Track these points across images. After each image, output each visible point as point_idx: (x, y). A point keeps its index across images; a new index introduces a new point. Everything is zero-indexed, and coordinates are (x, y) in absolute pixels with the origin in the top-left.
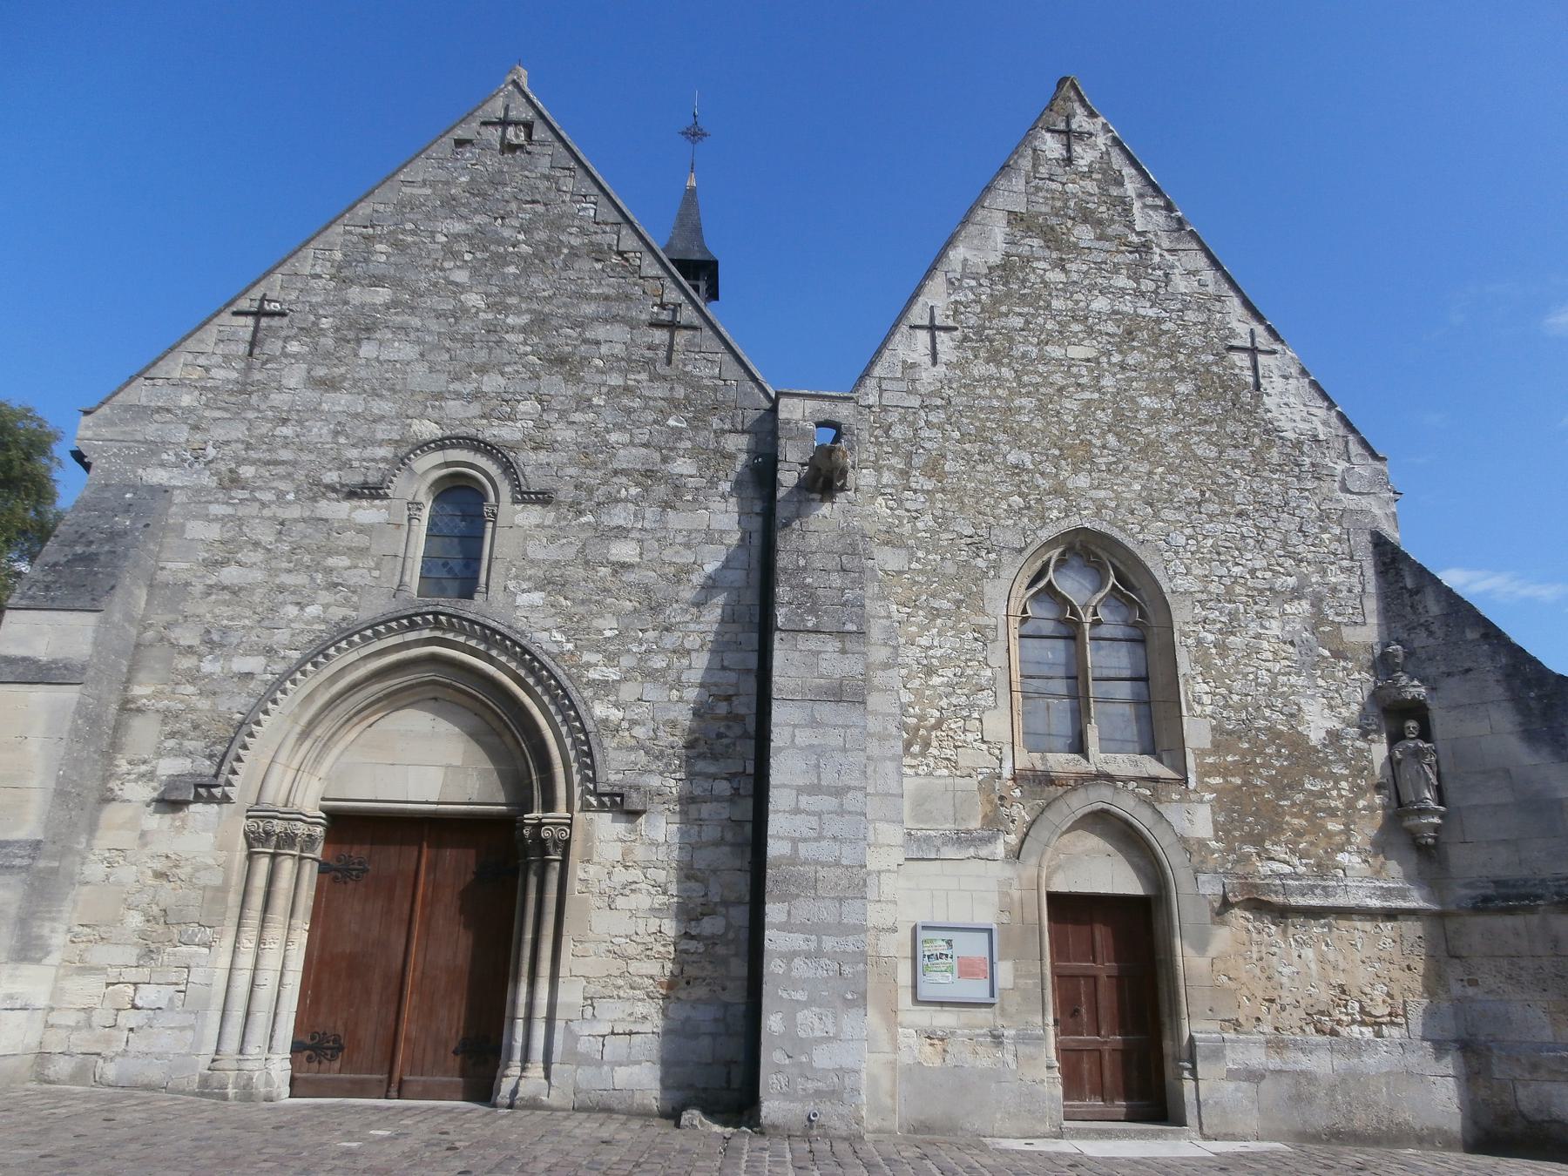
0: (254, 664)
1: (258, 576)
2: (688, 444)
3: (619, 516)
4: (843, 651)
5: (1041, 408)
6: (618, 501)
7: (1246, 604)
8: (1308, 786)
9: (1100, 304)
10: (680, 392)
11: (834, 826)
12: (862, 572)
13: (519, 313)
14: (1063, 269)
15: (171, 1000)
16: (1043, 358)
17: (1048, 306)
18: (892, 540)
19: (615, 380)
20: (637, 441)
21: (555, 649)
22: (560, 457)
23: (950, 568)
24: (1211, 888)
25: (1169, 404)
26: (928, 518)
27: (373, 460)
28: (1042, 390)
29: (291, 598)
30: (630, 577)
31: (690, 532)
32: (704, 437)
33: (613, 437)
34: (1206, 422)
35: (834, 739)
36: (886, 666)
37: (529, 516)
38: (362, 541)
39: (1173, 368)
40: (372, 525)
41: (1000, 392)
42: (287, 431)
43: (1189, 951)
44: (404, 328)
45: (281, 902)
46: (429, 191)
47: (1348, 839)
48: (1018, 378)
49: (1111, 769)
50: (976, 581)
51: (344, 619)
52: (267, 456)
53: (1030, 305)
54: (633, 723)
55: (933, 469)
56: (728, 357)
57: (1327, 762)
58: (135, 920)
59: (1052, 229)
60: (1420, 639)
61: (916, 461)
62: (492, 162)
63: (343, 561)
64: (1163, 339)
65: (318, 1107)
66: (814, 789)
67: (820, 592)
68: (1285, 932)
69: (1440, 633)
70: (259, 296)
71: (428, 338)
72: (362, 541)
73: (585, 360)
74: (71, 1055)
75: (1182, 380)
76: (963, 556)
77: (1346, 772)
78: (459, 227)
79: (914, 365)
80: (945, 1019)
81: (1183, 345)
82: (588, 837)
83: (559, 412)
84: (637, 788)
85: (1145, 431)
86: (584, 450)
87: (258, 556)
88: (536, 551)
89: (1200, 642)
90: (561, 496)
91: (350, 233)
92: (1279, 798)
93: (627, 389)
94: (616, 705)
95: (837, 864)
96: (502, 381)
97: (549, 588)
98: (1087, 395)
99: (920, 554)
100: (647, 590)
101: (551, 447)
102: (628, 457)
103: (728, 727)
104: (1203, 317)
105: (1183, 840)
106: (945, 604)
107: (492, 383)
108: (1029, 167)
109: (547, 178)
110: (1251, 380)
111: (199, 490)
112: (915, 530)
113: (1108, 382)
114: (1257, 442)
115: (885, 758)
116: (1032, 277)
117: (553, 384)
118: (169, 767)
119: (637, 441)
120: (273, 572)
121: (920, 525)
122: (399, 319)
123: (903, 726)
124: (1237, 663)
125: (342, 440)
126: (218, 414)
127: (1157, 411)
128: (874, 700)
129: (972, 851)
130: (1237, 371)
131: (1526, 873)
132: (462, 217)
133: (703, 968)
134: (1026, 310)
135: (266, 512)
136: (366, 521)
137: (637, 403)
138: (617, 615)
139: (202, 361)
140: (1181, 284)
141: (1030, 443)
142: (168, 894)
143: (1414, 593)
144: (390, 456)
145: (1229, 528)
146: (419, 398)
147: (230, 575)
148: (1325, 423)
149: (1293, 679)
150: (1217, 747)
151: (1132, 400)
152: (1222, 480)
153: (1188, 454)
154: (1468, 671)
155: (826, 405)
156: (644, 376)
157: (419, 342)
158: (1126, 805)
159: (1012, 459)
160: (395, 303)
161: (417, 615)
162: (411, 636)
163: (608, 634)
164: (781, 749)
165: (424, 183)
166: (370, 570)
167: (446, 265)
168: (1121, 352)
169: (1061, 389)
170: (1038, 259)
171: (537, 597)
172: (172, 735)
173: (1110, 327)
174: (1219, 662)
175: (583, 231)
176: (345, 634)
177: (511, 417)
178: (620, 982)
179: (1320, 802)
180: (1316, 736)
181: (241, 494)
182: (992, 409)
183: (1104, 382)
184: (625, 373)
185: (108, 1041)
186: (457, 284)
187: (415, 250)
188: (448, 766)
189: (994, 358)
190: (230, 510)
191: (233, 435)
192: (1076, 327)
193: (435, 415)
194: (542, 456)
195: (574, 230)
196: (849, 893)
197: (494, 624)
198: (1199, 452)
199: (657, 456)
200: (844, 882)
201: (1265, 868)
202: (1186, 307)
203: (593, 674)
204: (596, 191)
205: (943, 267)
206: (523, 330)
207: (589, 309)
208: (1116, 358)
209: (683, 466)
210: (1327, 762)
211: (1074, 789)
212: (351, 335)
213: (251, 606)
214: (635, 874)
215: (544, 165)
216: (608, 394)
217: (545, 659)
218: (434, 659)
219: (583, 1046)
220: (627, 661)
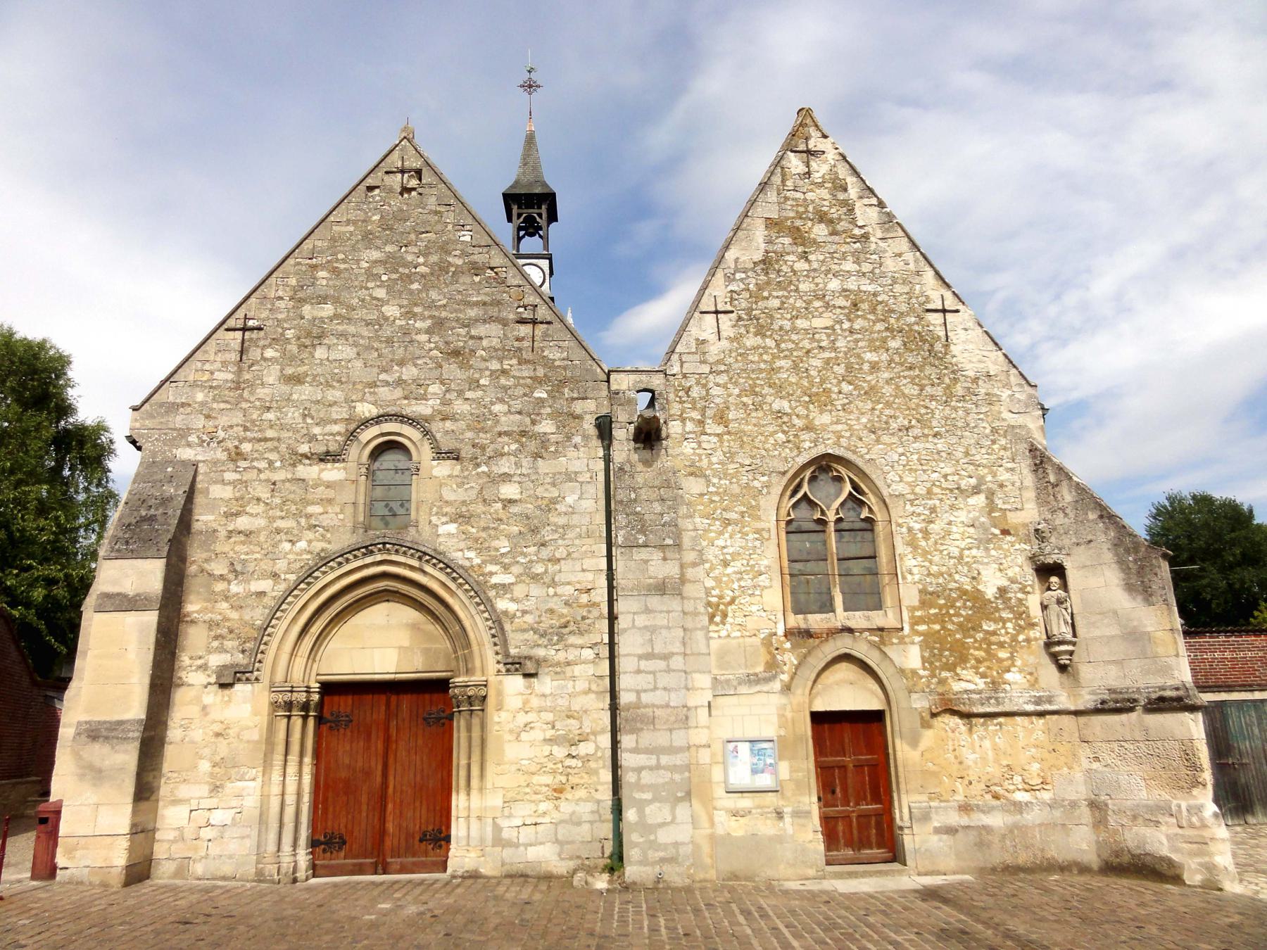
0: (265, 585)
1: (262, 522)
2: (549, 410)
3: (504, 466)
4: (665, 559)
5: (795, 367)
6: (502, 455)
7: (941, 500)
8: (985, 627)
9: (834, 284)
10: (541, 372)
11: (664, 680)
12: (675, 499)
13: (424, 319)
14: (807, 259)
15: (233, 819)
16: (794, 329)
17: (797, 290)
18: (696, 472)
19: (495, 365)
20: (513, 410)
21: (467, 564)
22: (462, 425)
23: (736, 489)
24: (921, 703)
25: (885, 357)
26: (719, 453)
28: (795, 354)
29: (284, 537)
30: (515, 509)
31: (554, 474)
32: (561, 404)
33: (497, 408)
34: (910, 368)
35: (661, 620)
36: (694, 565)
37: (443, 469)
38: (330, 494)
39: (887, 329)
40: (335, 482)
41: (765, 357)
42: (270, 416)
43: (906, 748)
44: (343, 335)
45: (295, 747)
46: (351, 228)
48: (778, 345)
49: (852, 624)
50: (754, 497)
51: (323, 550)
52: (259, 435)
53: (785, 289)
54: (524, 612)
55: (721, 418)
56: (573, 344)
57: (997, 610)
58: (205, 766)
59: (798, 229)
60: (1060, 519)
61: (709, 413)
62: (396, 202)
63: (316, 509)
64: (879, 307)
65: (335, 885)
66: (649, 656)
67: (646, 517)
68: (970, 730)
69: (1072, 515)
70: (242, 316)
71: (362, 342)
72: (330, 494)
73: (473, 351)
74: (174, 860)
75: (893, 338)
76: (744, 480)
78: (376, 255)
79: (704, 342)
80: (745, 802)
81: (893, 311)
82: (500, 693)
84: (530, 658)
85: (868, 378)
86: (480, 419)
87: (260, 508)
88: (448, 495)
89: (910, 530)
90: (463, 454)
91: (299, 264)
92: (965, 637)
93: (504, 372)
94: (512, 600)
95: (667, 706)
96: (414, 371)
98: (827, 355)
99: (715, 480)
100: (528, 518)
102: (508, 422)
103: (589, 612)
104: (906, 289)
105: (902, 671)
106: (733, 516)
107: (409, 372)
108: (779, 183)
109: (436, 213)
110: (942, 334)
111: (215, 463)
112: (711, 463)
113: (841, 343)
114: (947, 380)
115: (697, 629)
116: (784, 268)
117: (452, 370)
118: (216, 660)
119: (513, 410)
120: (272, 519)
121: (714, 460)
122: (340, 328)
123: (709, 604)
124: (936, 543)
125: (309, 421)
126: (222, 406)
127: (877, 363)
128: (689, 589)
129: (758, 688)
130: (931, 328)
131: (1128, 683)
132: (378, 248)
133: (582, 778)
134: (781, 293)
135: (262, 476)
137: (511, 382)
138: (508, 537)
139: (207, 367)
140: (891, 265)
141: (789, 394)
142: (223, 748)
143: (1055, 486)
144: (343, 430)
145: (928, 445)
146: (359, 387)
147: (242, 523)
148: (995, 363)
149: (974, 552)
150: (924, 604)
151: (858, 356)
152: (923, 411)
153: (899, 393)
154: (1090, 541)
155: (644, 377)
156: (514, 361)
157: (355, 345)
158: (860, 649)
159: (776, 406)
160: (336, 316)
162: (369, 560)
163: (503, 551)
164: (625, 630)
165: (348, 222)
167: (370, 285)
168: (849, 320)
169: (808, 352)
170: (788, 254)
171: (452, 528)
172: (216, 638)
173: (841, 302)
174: (923, 543)
175: (464, 254)
176: (325, 561)
177: (424, 397)
178: (527, 790)
179: (993, 639)
180: (990, 592)
181: (243, 464)
182: (761, 371)
183: (838, 344)
184: (501, 360)
185: (196, 849)
186: (378, 299)
187: (346, 275)
188: (400, 648)
189: (760, 332)
190: (238, 476)
191: (235, 421)
192: (817, 304)
193: (372, 399)
194: (448, 424)
195: (458, 253)
196: (676, 726)
197: (423, 549)
198: (906, 391)
199: (528, 420)
200: (673, 718)
201: (957, 687)
202: (894, 281)
203: (494, 580)
204: (470, 221)
205: (722, 266)
206: (429, 331)
207: (472, 313)
208: (846, 325)
209: (547, 427)
210: (997, 610)
211: (827, 640)
212: (308, 342)
213: (259, 544)
214: (531, 717)
215: (432, 202)
216: (491, 375)
217: (461, 571)
219: (505, 834)
220: (516, 570)
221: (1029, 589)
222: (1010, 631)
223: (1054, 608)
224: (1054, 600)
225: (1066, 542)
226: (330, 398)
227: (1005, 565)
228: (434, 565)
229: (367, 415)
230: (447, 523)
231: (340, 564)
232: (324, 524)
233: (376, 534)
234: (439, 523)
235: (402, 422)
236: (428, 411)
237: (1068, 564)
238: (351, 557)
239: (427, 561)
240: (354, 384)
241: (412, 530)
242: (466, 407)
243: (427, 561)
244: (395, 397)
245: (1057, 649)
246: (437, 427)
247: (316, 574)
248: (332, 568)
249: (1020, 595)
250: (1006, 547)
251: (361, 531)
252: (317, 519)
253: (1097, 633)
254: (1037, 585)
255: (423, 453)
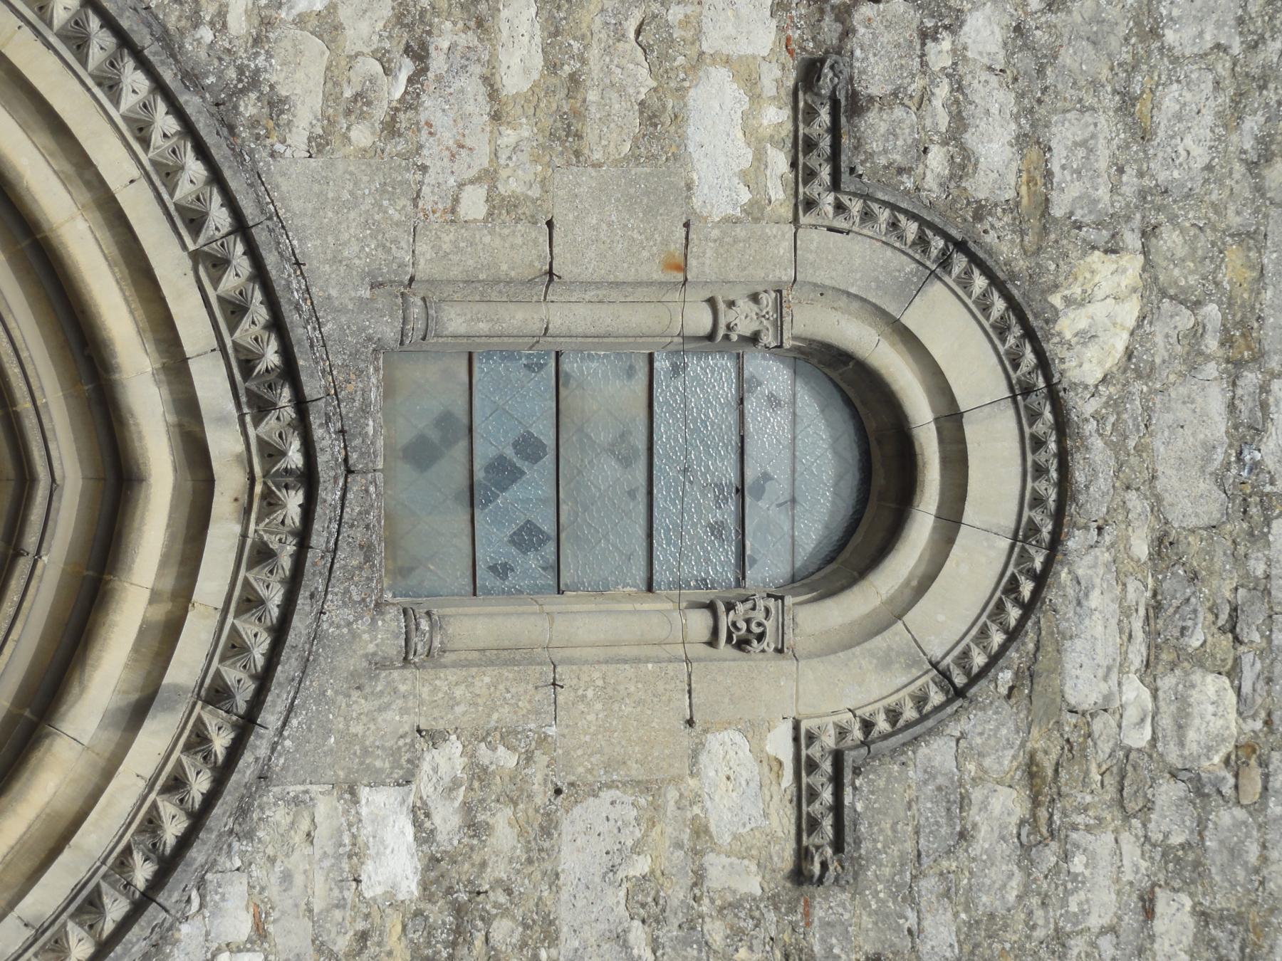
22: (1000, 884)
27: (959, 122)
37: (742, 795)
38: (611, 133)
40: (679, 157)
51: (276, 105)
63: (520, 59)
72: (611, 133)
83: (1196, 845)
97: (439, 914)
101: (1042, 830)
136: (695, 133)
144: (981, 186)
146: (1234, 268)
161: (301, 404)
162: (212, 384)
166: (489, 177)
171: (395, 868)
177: (1162, 654)
194: (1003, 806)
197: (270, 717)
218: (117, 479)
226: (1170, 99)
228: (176, 784)
229: (1069, 324)
230: (424, 835)
231: (194, 220)
232: (430, 106)
233: (376, 416)
234: (425, 785)
235: (1024, 534)
236: (1082, 687)
238: (231, 282)
239: (198, 741)
240: (1250, 238)
241: (383, 635)
242: (1100, 903)
243: (198, 741)
244: (1169, 480)
246: (992, 733)
247: (135, 82)
248: (169, 174)
251: (388, 330)
252: (462, 60)
255: (838, 671)
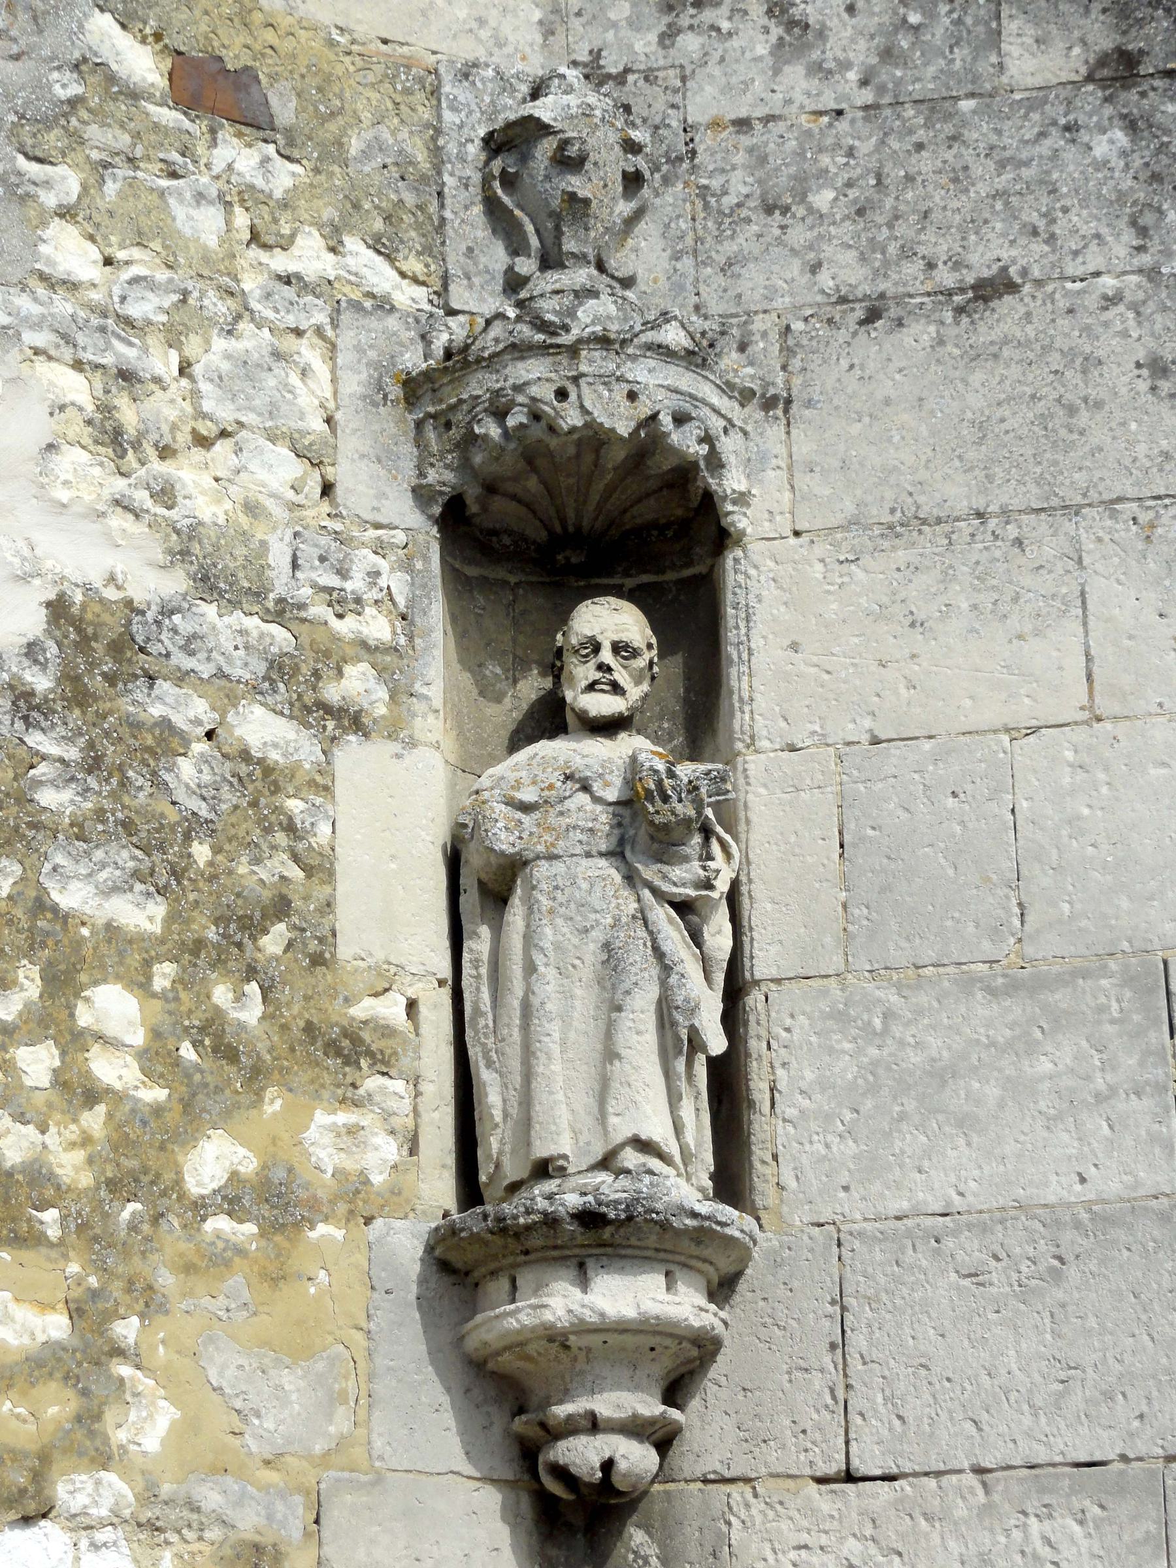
47: (89, 1419)
77: (143, 915)
154: (993, 289)
221: (357, 684)
222: (111, 1070)
223: (580, 895)
224: (589, 815)
225: (772, 281)
227: (166, 409)
237: (762, 490)
245: (560, 1301)
249: (262, 728)
250: (204, 226)
253: (950, 1173)
254: (436, 667)
